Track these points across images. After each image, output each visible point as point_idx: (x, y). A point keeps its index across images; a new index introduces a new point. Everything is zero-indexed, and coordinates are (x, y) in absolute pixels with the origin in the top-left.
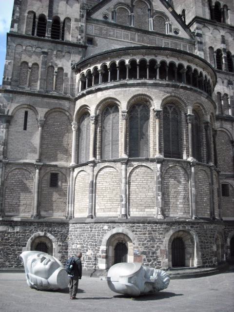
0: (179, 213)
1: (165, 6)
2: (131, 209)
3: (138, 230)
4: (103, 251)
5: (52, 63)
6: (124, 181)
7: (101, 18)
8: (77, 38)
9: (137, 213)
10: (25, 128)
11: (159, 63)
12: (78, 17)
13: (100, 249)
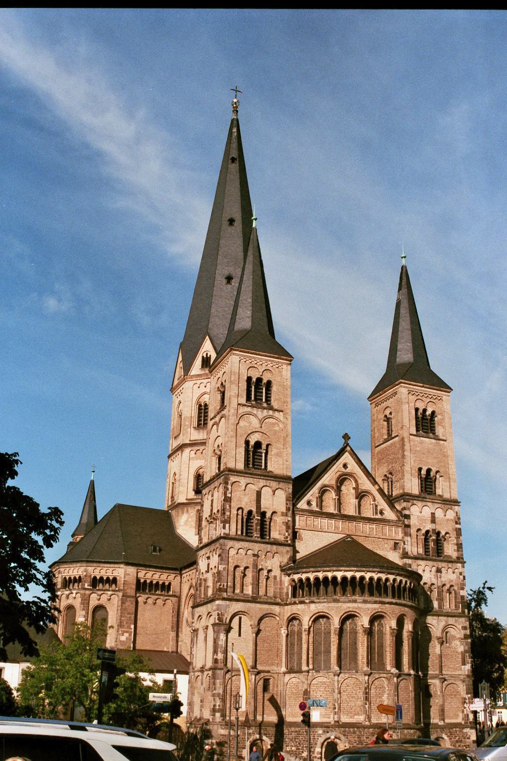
0: (383, 720)
1: (372, 483)
2: (342, 716)
4: (318, 752)
5: (262, 565)
6: (336, 691)
7: (305, 507)
8: (284, 535)
10: (240, 635)
11: (367, 580)
12: (285, 511)
13: (316, 751)
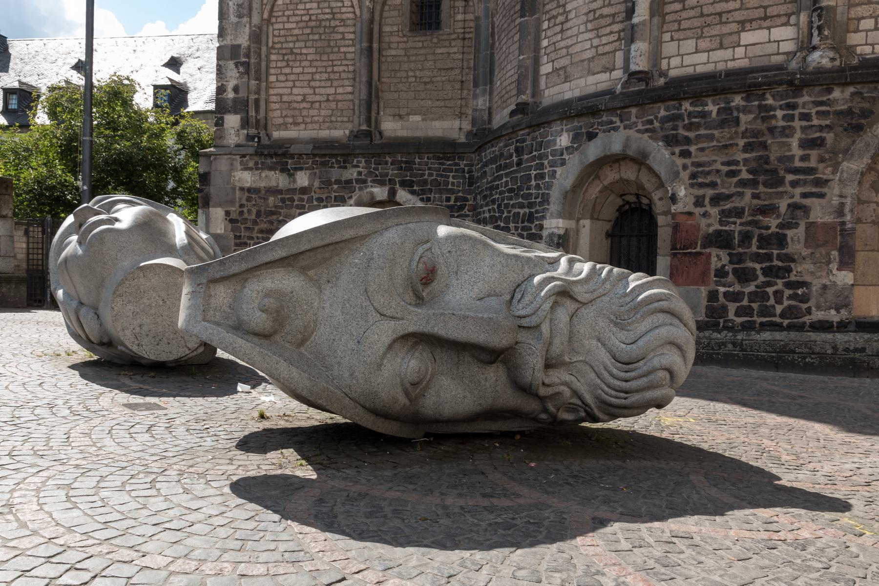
2: (669, 48)
3: (691, 135)
9: (703, 57)
